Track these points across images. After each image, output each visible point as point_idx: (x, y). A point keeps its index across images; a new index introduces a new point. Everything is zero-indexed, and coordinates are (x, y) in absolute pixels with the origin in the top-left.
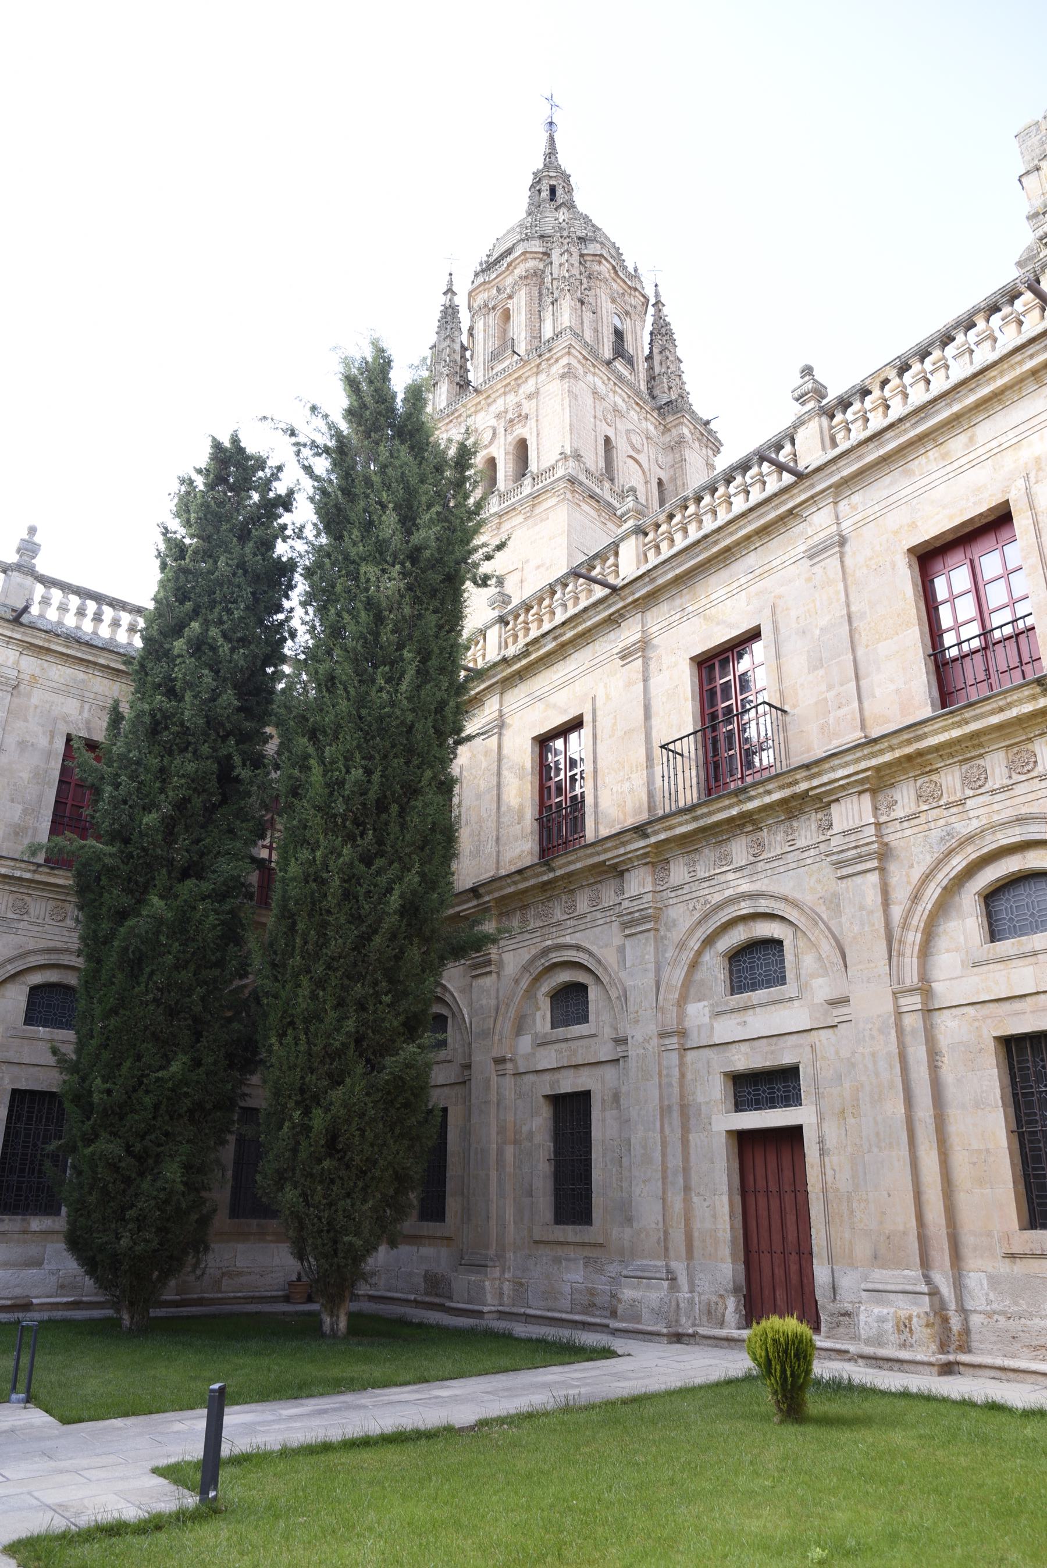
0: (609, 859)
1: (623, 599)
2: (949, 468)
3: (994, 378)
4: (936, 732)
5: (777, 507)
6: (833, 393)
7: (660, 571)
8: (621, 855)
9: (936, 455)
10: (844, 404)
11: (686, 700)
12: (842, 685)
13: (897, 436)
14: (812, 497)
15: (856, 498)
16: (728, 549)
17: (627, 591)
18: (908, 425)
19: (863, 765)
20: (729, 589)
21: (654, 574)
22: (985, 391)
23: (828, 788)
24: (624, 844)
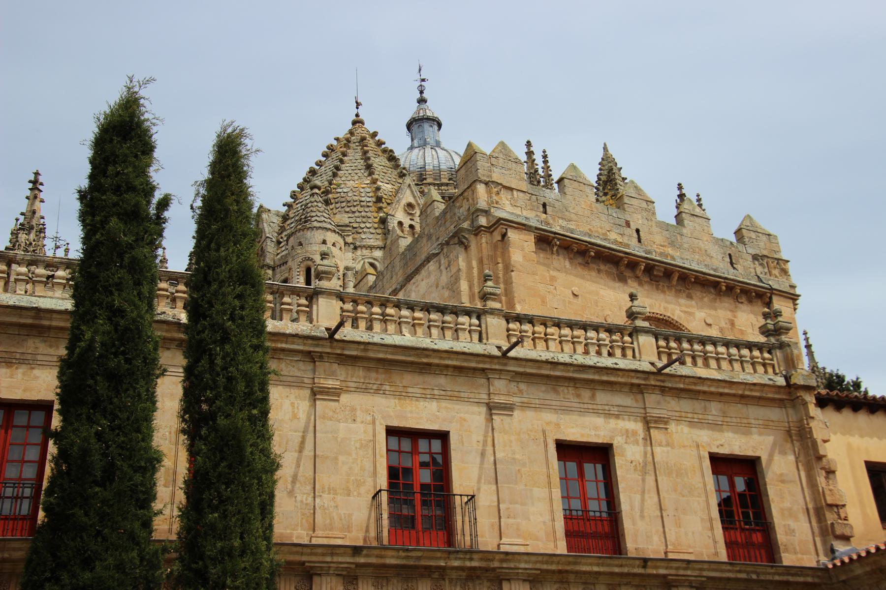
0: (309, 562)
1: (331, 347)
2: (582, 406)
3: (618, 376)
4: (586, 564)
5: (478, 362)
6: (519, 309)
7: (375, 348)
8: (327, 562)
9: (573, 392)
10: (520, 319)
11: (382, 456)
12: (511, 503)
13: (563, 371)
14: (501, 370)
15: (523, 386)
16: (429, 364)
17: (340, 344)
18: (572, 369)
19: (538, 566)
20: (424, 392)
21: (370, 347)
22: (612, 379)
23: (511, 571)
24: (332, 555)
